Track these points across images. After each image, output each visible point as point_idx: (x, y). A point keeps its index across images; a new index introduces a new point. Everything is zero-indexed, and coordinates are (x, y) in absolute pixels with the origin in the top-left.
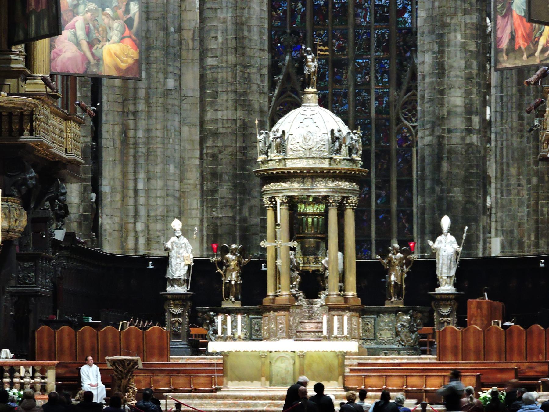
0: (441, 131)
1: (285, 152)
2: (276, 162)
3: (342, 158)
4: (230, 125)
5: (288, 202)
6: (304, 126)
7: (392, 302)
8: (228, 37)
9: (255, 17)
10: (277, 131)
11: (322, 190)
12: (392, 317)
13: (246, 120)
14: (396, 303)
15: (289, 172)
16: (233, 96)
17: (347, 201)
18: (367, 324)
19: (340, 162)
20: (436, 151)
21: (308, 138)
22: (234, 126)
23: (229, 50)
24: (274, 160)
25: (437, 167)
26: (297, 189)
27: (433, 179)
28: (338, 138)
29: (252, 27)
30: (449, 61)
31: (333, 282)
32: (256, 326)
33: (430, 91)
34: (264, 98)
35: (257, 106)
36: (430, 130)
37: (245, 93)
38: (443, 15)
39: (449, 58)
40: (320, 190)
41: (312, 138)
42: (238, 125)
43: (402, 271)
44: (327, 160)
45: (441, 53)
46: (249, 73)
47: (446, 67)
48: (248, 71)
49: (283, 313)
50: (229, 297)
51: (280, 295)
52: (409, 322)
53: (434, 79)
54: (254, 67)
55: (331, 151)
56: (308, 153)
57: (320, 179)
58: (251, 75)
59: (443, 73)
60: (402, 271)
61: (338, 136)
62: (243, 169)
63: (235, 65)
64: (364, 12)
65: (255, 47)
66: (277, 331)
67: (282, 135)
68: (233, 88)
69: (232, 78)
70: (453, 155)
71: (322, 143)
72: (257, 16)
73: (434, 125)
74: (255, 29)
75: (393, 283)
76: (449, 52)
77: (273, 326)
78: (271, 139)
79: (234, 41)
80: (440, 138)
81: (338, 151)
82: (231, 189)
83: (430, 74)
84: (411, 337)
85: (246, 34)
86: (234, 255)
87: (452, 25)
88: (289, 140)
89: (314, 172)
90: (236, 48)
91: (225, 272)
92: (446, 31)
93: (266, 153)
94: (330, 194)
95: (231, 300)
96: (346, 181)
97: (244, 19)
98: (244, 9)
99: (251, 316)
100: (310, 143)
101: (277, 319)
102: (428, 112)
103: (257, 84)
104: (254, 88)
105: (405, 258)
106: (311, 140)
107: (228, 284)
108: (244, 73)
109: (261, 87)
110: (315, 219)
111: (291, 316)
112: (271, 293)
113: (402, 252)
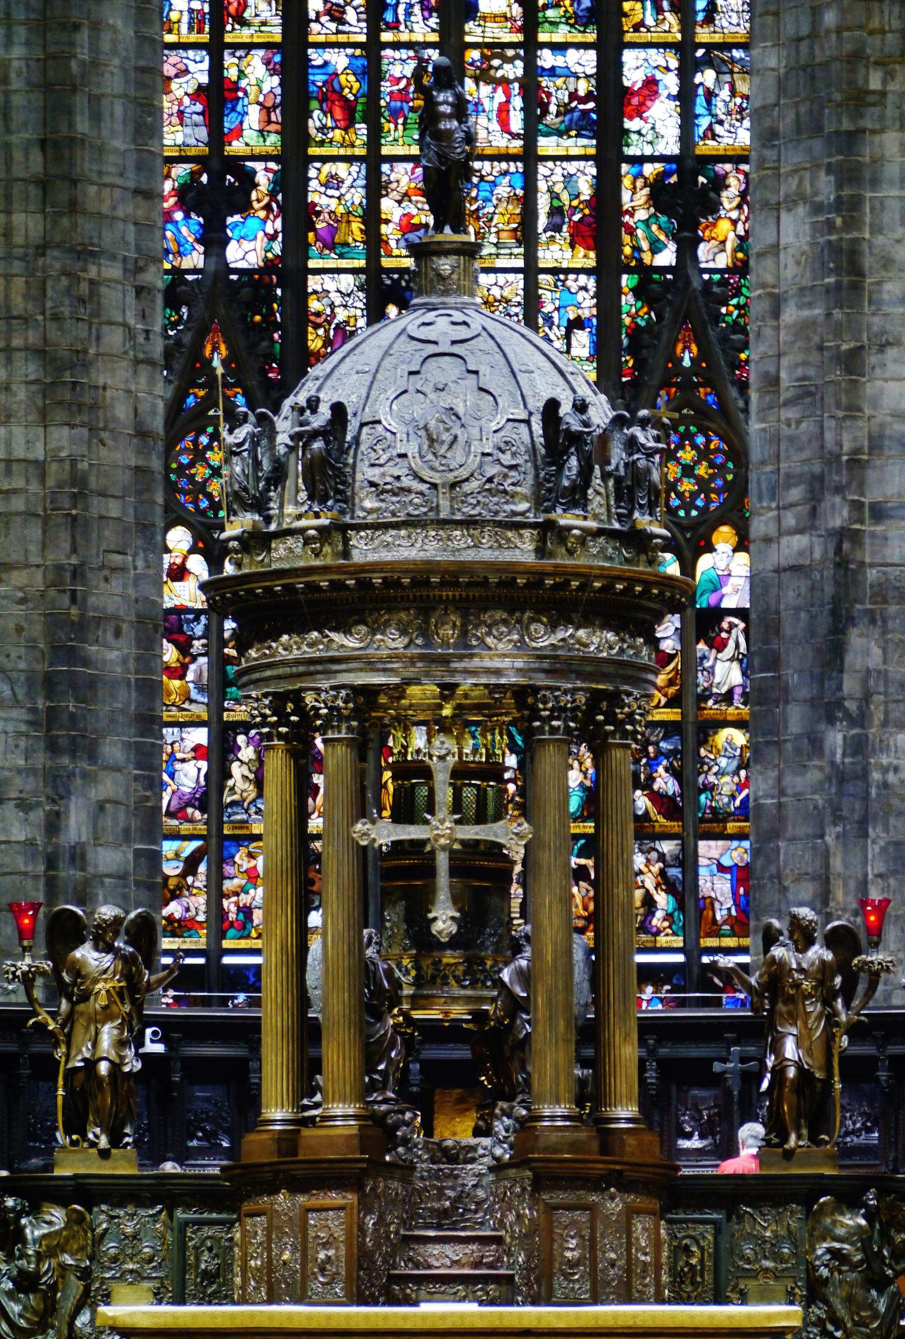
0: (845, 513)
1: (347, 500)
2: (307, 541)
3: (592, 524)
4: (18, 483)
5: (357, 713)
6: (428, 389)
7: (789, 1155)
8: (14, 139)
9: (116, 62)
10: (313, 404)
11: (506, 663)
12: (793, 1218)
13: (83, 465)
14: (807, 1160)
15: (364, 585)
16: (32, 370)
17: (611, 718)
18: (687, 1248)
19: (582, 541)
20: (829, 590)
21: (446, 437)
22: (34, 487)
23: (16, 189)
24: (302, 531)
25: (833, 654)
26: (397, 657)
27: (812, 703)
28: (576, 439)
29: (105, 103)
30: (880, 240)
31: (552, 1063)
32: (206, 1256)
33: (800, 358)
34: (152, 381)
35: (122, 412)
36: (804, 509)
37: (80, 360)
38: (856, 58)
39: (877, 229)
40: (497, 664)
41: (462, 439)
42: (51, 482)
43: (831, 1019)
44: (526, 533)
45: (849, 208)
46: (92, 282)
47: (867, 262)
48: (93, 272)
49: (334, 1198)
50: (84, 1135)
51: (325, 1118)
52: (863, 1238)
53: (818, 311)
54: (113, 257)
55: (547, 495)
56: (444, 503)
57: (500, 615)
58: (104, 290)
59: (856, 287)
60: (831, 1019)
61: (576, 427)
62: (73, 656)
63: (42, 249)
64: (500, 97)
65: (118, 181)
66: (306, 1277)
67: (330, 422)
68: (33, 337)
69: (26, 296)
70: (893, 609)
71: (507, 459)
72: (126, 60)
73: (817, 488)
74: (119, 111)
75: (791, 1073)
76: (879, 206)
77: (286, 1256)
78: (283, 439)
79: (36, 156)
80: (846, 536)
81: (576, 497)
82: (19, 734)
83: (802, 290)
84: (871, 1306)
85: (82, 125)
86: (109, 949)
87: (890, 98)
88: (363, 448)
89: (469, 585)
90: (44, 184)
91: (70, 1019)
92: (868, 123)
93: (259, 505)
94: (541, 680)
95: (93, 1145)
96: (606, 626)
97: (74, 66)
98: (77, 27)
99: (179, 1214)
100: (457, 456)
101: (304, 1227)
102: (791, 439)
103: (125, 325)
104: (114, 339)
105: (842, 966)
106: (459, 448)
107: (81, 1076)
108: (73, 277)
109: (141, 339)
110: (469, 794)
111: (369, 1211)
112: (276, 1112)
113: (833, 939)
